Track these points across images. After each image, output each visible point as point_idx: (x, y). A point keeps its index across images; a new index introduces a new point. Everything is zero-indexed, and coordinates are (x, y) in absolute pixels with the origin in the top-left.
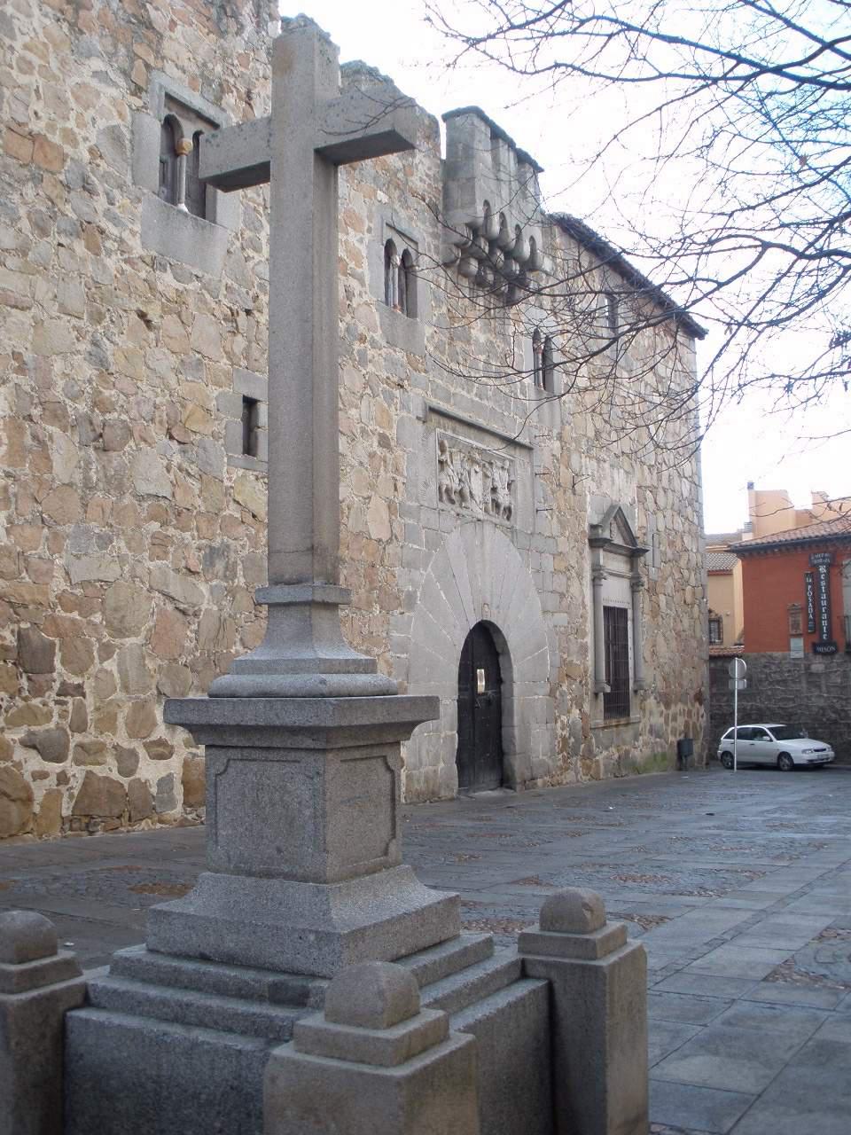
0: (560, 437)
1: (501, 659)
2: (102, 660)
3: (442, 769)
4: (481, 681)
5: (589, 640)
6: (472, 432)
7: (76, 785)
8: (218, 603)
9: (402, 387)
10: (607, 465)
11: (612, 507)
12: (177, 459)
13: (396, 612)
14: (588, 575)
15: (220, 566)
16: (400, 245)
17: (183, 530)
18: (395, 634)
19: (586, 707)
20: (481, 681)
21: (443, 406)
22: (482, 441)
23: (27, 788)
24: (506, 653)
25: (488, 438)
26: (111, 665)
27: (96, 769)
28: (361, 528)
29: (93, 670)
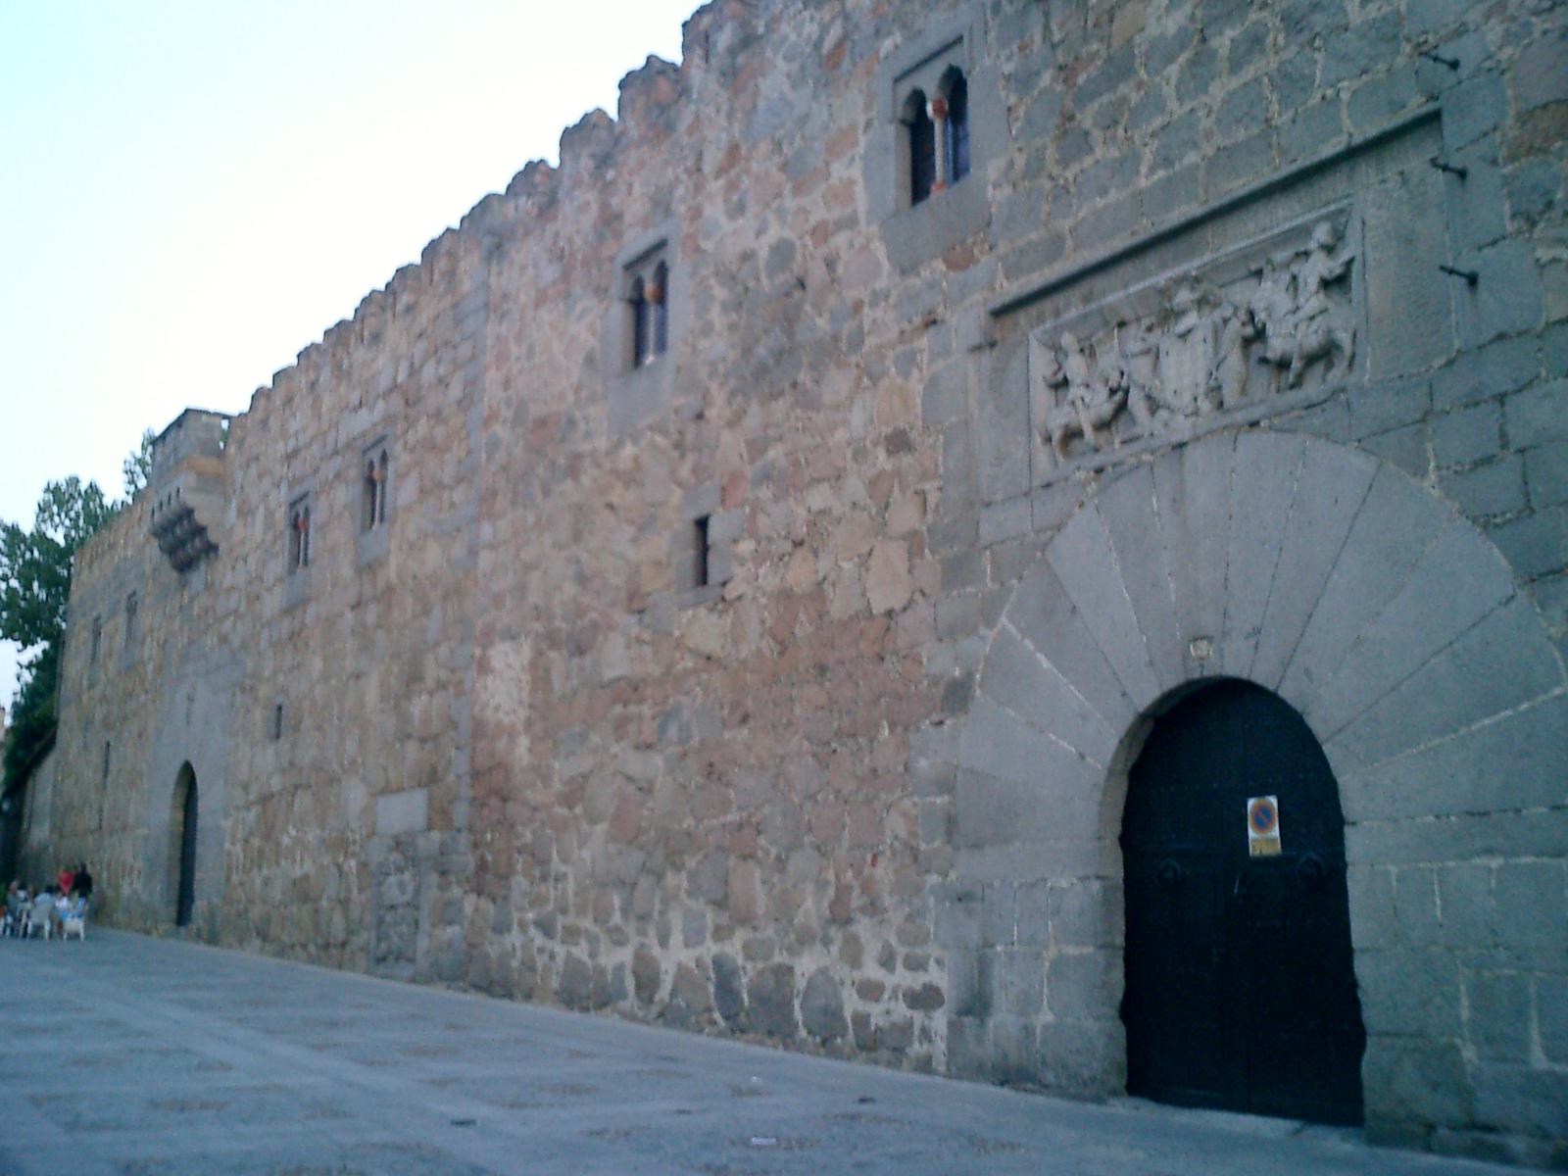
2: (580, 847)
3: (1045, 1028)
4: (1262, 825)
6: (1151, 260)
7: (560, 961)
9: (934, 322)
15: (673, 731)
17: (641, 701)
20: (1262, 825)
23: (533, 960)
25: (1209, 233)
26: (586, 854)
28: (858, 605)
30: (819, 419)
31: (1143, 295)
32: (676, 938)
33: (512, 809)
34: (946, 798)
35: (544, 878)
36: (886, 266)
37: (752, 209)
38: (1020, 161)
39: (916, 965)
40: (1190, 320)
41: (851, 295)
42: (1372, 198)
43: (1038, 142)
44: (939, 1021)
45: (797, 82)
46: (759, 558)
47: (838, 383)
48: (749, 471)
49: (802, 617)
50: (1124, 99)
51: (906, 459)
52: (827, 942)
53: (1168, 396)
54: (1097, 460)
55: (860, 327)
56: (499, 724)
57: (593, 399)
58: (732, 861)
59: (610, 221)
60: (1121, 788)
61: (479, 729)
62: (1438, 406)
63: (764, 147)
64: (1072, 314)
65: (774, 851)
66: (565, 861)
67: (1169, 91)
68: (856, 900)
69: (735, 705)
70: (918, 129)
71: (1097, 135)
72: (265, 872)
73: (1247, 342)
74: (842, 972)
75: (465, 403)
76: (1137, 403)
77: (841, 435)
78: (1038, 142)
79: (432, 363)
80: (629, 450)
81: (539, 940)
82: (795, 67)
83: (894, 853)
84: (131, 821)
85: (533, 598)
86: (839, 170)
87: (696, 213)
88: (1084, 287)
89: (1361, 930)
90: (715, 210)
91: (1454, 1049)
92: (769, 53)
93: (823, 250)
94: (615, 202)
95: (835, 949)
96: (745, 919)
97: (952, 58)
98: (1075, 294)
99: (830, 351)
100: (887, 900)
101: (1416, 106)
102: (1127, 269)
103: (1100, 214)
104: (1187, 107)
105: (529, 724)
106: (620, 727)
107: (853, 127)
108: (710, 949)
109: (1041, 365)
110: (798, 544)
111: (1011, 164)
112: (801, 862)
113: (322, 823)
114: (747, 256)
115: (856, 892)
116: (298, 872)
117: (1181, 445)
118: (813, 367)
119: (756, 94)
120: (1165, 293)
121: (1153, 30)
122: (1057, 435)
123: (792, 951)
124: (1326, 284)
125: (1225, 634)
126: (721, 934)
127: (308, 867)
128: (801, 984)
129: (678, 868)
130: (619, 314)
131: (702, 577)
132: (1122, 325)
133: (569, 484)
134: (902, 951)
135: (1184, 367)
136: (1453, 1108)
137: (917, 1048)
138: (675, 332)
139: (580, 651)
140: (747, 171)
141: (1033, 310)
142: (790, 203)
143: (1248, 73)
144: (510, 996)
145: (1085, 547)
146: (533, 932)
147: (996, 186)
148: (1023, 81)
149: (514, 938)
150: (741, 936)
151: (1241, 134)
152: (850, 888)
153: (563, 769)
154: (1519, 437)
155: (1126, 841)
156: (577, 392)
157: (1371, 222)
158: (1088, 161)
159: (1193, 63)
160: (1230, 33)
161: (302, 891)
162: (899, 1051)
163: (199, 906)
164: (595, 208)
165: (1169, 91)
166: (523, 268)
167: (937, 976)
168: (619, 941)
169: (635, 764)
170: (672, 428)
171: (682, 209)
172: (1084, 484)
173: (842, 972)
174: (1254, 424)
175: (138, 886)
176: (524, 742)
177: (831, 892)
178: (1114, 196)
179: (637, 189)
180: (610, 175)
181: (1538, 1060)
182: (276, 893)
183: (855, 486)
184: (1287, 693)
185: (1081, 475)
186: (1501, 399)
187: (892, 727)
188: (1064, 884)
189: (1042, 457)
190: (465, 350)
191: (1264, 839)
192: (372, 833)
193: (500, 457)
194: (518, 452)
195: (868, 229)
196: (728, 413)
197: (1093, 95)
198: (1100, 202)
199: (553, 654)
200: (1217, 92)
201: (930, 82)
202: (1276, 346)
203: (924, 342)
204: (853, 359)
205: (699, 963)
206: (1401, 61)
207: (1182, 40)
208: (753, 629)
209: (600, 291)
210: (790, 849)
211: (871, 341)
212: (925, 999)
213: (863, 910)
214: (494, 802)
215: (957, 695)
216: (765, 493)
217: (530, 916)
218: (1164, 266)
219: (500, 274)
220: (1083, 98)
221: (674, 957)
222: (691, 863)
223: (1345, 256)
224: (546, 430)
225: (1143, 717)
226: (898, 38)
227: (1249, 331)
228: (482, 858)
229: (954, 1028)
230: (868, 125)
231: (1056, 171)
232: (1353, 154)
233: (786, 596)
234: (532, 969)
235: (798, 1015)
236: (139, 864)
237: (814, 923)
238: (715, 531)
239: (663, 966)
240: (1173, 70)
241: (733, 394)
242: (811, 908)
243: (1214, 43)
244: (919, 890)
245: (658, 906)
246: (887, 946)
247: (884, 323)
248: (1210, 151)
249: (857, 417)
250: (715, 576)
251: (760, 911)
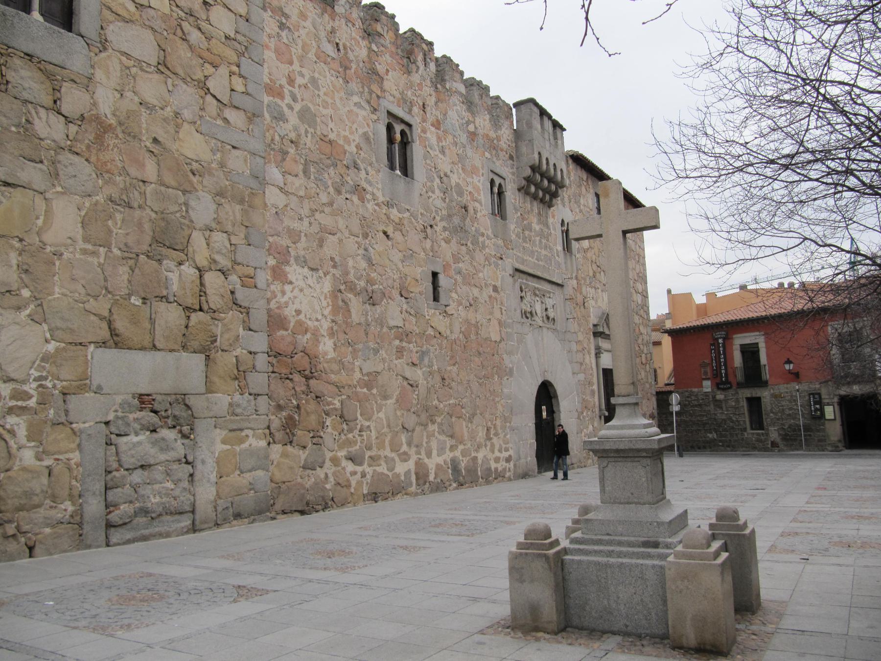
0: (577, 278)
1: (553, 400)
2: (378, 412)
5: (595, 387)
6: (535, 280)
8: (426, 379)
10: (600, 291)
11: (603, 314)
12: (405, 306)
14: (593, 352)
16: (498, 181)
17: (409, 343)
18: (505, 390)
19: (596, 424)
21: (522, 268)
23: (348, 481)
24: (556, 396)
25: (543, 282)
27: (377, 468)
29: (374, 418)
32: (435, 452)
39: (507, 450)
44: (512, 464)
52: (486, 446)
56: (300, 323)
66: (369, 419)
68: (492, 432)
74: (491, 456)
81: (350, 467)
95: (488, 448)
96: (461, 442)
100: (500, 431)
101: (560, 282)
106: (400, 351)
108: (448, 455)
112: (477, 419)
123: (477, 451)
126: (453, 448)
128: (480, 462)
129: (433, 422)
134: (504, 446)
137: (508, 474)
144: (326, 508)
146: (344, 463)
149: (329, 468)
150: (461, 447)
162: (504, 477)
167: (511, 452)
168: (405, 457)
169: (409, 372)
205: (445, 461)
208: (457, 329)
212: (508, 460)
217: (342, 454)
221: (432, 463)
222: (439, 420)
229: (515, 465)
237: (482, 441)
238: (442, 280)
239: (430, 467)
242: (481, 434)
245: (425, 440)
246: (500, 445)
251: (466, 438)
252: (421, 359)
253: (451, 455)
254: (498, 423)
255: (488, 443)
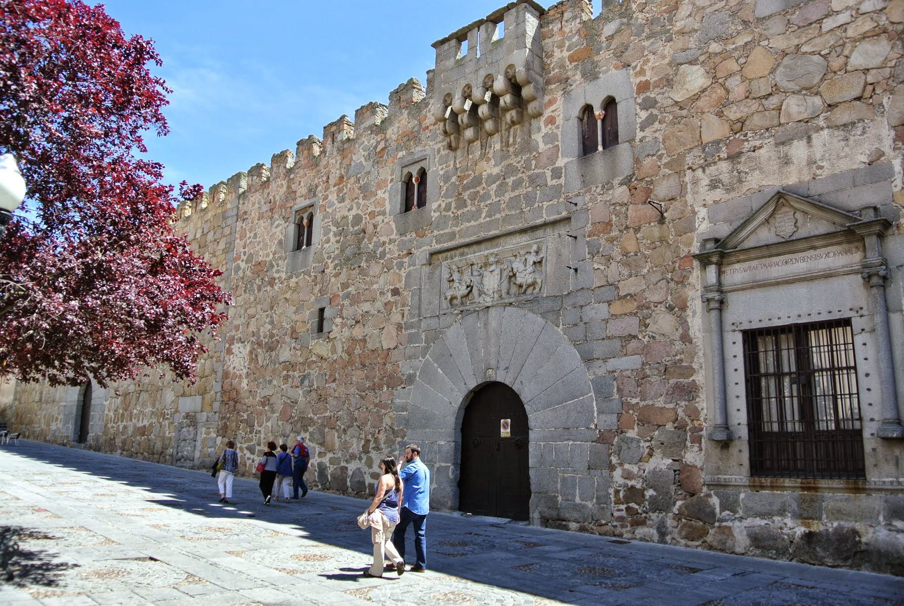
6: (483, 246)
13: (399, 388)
15: (306, 382)
17: (294, 371)
18: (397, 401)
20: (505, 428)
22: (497, 246)
25: (502, 240)
26: (269, 424)
28: (378, 345)
30: (368, 279)
31: (479, 257)
33: (238, 406)
34: (405, 413)
35: (251, 432)
36: (395, 231)
37: (347, 201)
38: (443, 205)
40: (493, 267)
41: (383, 239)
42: (551, 240)
43: (450, 200)
45: (368, 158)
46: (343, 325)
47: (375, 269)
48: (341, 294)
49: (358, 347)
50: (478, 192)
51: (396, 297)
52: (360, 459)
53: (485, 290)
54: (461, 309)
55: (385, 250)
56: (235, 373)
57: (280, 258)
58: (327, 430)
59: (291, 194)
60: (463, 412)
61: (226, 375)
62: (564, 306)
63: (352, 180)
64: (457, 259)
65: (343, 427)
67: (492, 193)
68: (372, 445)
69: (331, 375)
70: (408, 184)
71: (469, 201)
72: (124, 423)
73: (510, 277)
74: (365, 469)
75: (226, 251)
76: (475, 291)
77: (375, 286)
78: (450, 200)
79: (212, 232)
80: (294, 280)
81: (248, 455)
82: (366, 153)
83: (386, 429)
84: (57, 399)
85: (252, 328)
86: (380, 193)
87: (326, 198)
88: (461, 250)
89: (532, 461)
90: (333, 197)
91: (557, 497)
92: (357, 146)
93: (373, 221)
94: (293, 186)
95: (363, 461)
97: (422, 164)
98: (458, 252)
99: (372, 256)
100: (383, 446)
101: (564, 214)
102: (475, 247)
103: (467, 230)
104: (498, 199)
105: (248, 375)
106: (286, 378)
107: (386, 180)
109: (446, 276)
110: (358, 322)
111: (440, 205)
113: (154, 405)
114: (344, 217)
115: (372, 443)
116: (140, 424)
117: (488, 307)
118: (367, 261)
119: (351, 159)
120: (487, 257)
121: (489, 171)
122: (449, 298)
124: (535, 263)
125: (498, 368)
127: (146, 423)
128: (350, 473)
129: (306, 431)
130: (292, 229)
131: (320, 329)
132: (472, 265)
133: (269, 288)
135: (492, 281)
136: (554, 513)
138: (315, 239)
139: (271, 349)
140: (346, 187)
141: (444, 255)
142: (361, 201)
143: (517, 193)
145: (455, 334)
146: (245, 451)
147: (435, 211)
148: (446, 178)
150: (329, 455)
151: (513, 212)
152: (369, 441)
153: (262, 393)
154: (586, 320)
155: (463, 430)
156: (274, 254)
157: (550, 247)
158: (466, 210)
159: (500, 185)
160: (512, 178)
161: (143, 431)
163: (91, 435)
164: (285, 186)
165: (492, 193)
166: (254, 204)
169: (291, 393)
170: (313, 274)
171: (320, 195)
172: (458, 315)
173: (365, 469)
174: (511, 304)
175: (60, 426)
176: (245, 381)
177: (363, 442)
178: (473, 223)
179: (302, 184)
180: (292, 176)
181: (578, 500)
182: (130, 431)
183: (379, 305)
184: (515, 388)
185: (456, 312)
186: (582, 307)
187: (388, 387)
188: (443, 443)
189: (445, 304)
190: (227, 231)
191: (505, 432)
192: (177, 411)
193: (240, 273)
194: (248, 273)
195: (389, 218)
196: (334, 272)
197: (469, 188)
198: (468, 224)
199: (259, 350)
200: (507, 196)
201: (415, 170)
202: (519, 280)
203: (406, 260)
204: (382, 261)
206: (561, 200)
207: (497, 177)
209: (286, 219)
210: (349, 427)
211: (388, 256)
213: (373, 448)
214: (231, 403)
215: (411, 379)
216: (347, 302)
217: (245, 446)
218: (487, 249)
219: (244, 204)
220: (466, 188)
222: (311, 429)
223: (541, 256)
224: (260, 268)
225: (471, 392)
226: (404, 153)
227: (511, 274)
228: (225, 423)
230: (392, 180)
231: (455, 211)
232: (545, 225)
233: (353, 339)
234: (245, 465)
235: (349, 484)
236: (61, 417)
238: (327, 314)
240: (494, 186)
241: (336, 265)
242: (356, 447)
243: (507, 180)
244: (394, 443)
247: (393, 250)
248: (503, 214)
249: (381, 280)
250: (325, 329)
252: (302, 382)
253: (319, 460)
254: (382, 437)
255: (364, 457)
